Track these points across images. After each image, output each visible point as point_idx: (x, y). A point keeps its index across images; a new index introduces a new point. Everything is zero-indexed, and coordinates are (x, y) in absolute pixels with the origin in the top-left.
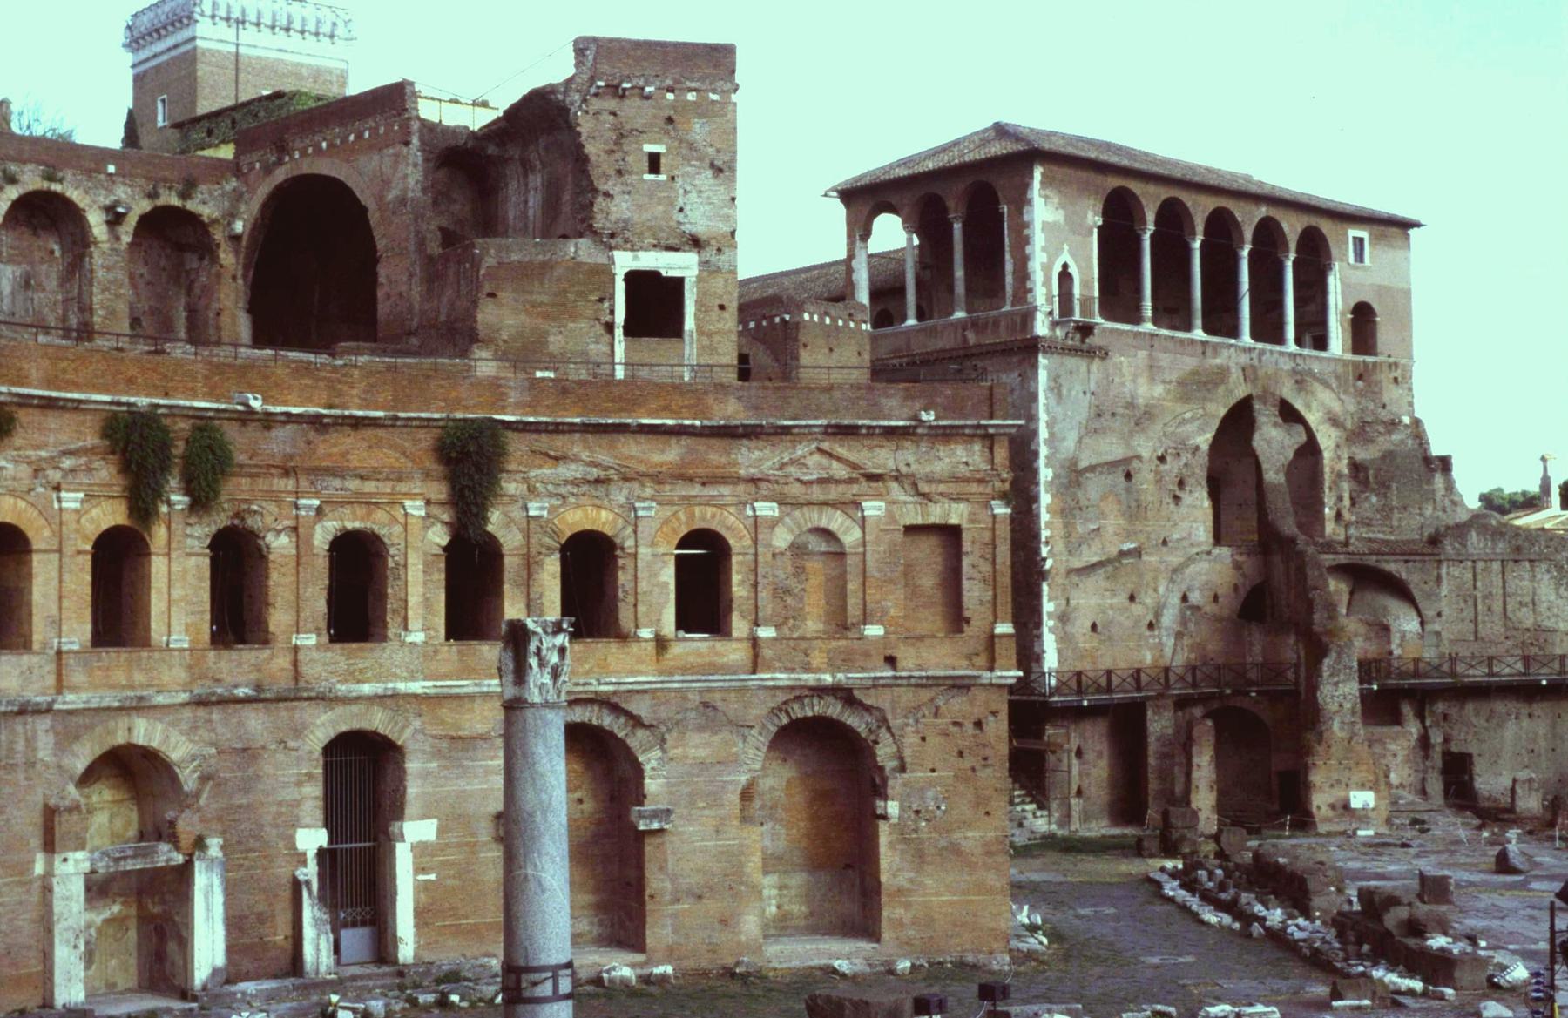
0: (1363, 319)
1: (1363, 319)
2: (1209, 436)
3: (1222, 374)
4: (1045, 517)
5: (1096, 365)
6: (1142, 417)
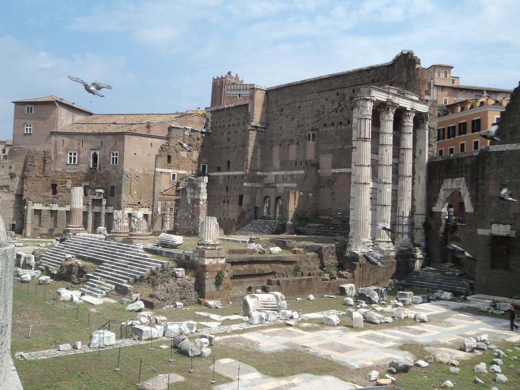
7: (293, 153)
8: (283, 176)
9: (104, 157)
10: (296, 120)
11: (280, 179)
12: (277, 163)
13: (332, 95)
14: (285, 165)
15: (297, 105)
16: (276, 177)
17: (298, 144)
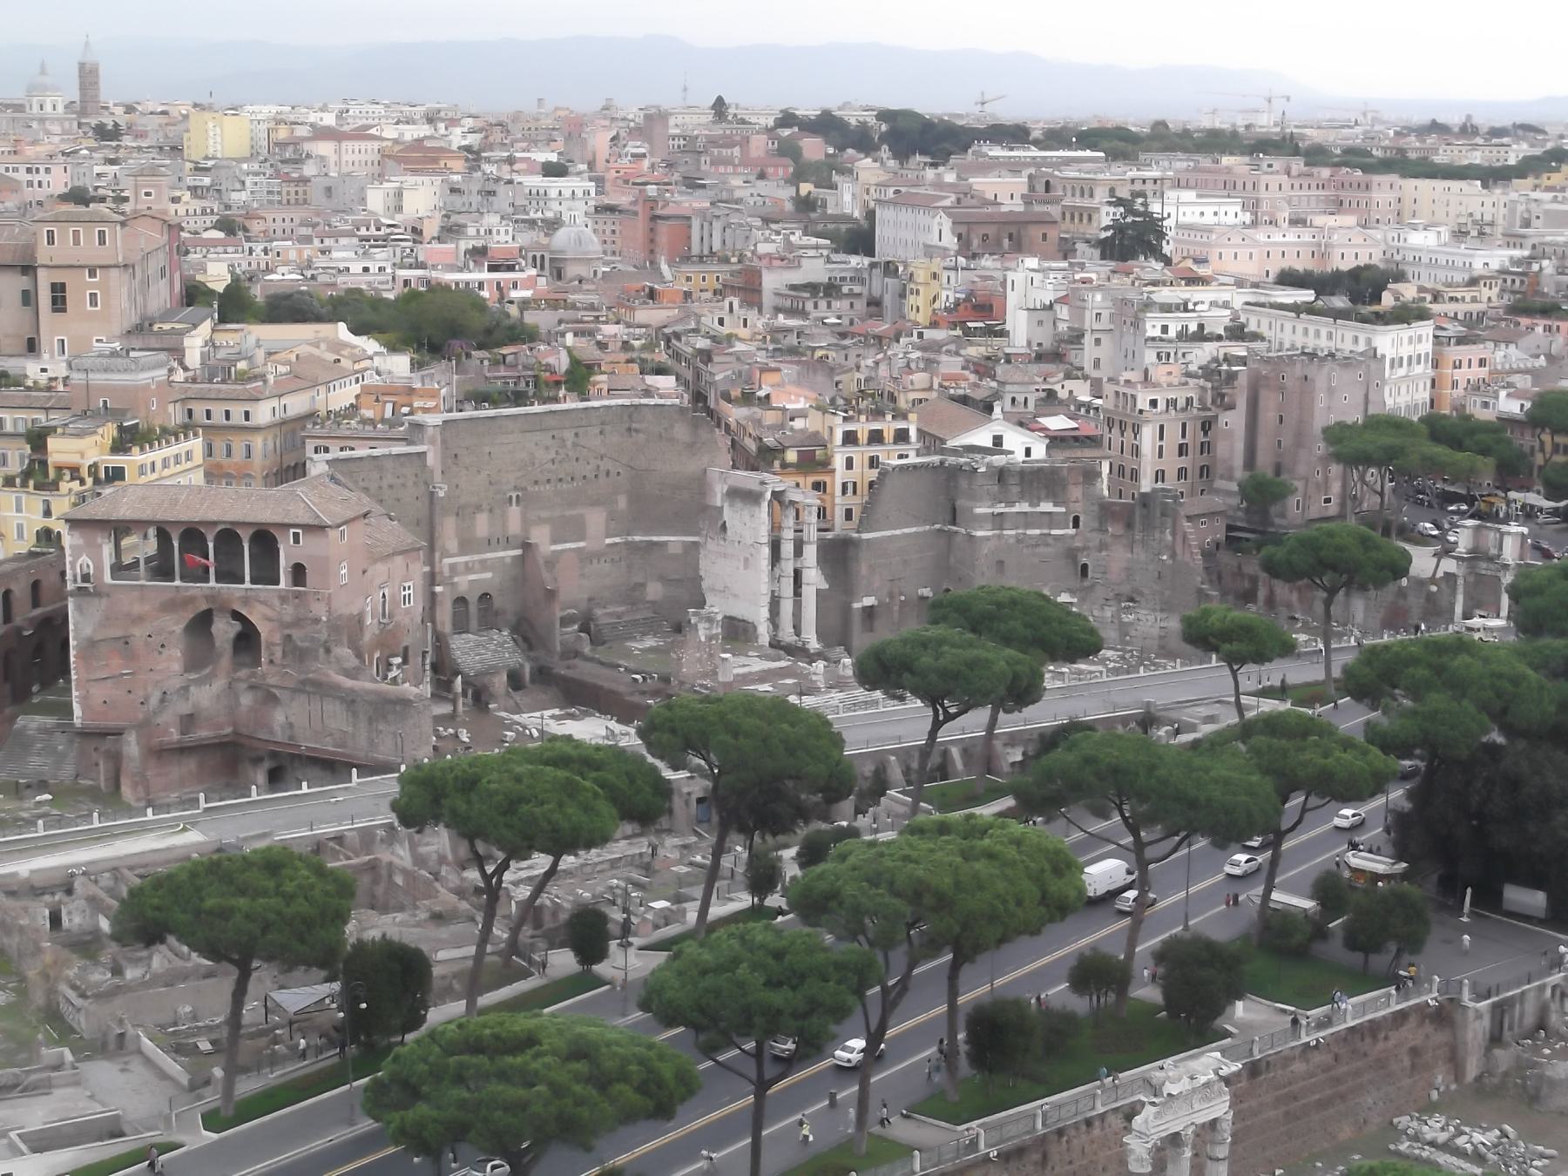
0: (299, 573)
1: (299, 573)
2: (182, 626)
3: (191, 600)
4: (72, 659)
5: (104, 601)
6: (139, 619)
7: (482, 525)
8: (466, 563)
9: (393, 596)
10: (484, 474)
11: (461, 568)
12: (452, 544)
13: (545, 439)
14: (466, 546)
15: (487, 449)
16: (453, 567)
17: (491, 511)
